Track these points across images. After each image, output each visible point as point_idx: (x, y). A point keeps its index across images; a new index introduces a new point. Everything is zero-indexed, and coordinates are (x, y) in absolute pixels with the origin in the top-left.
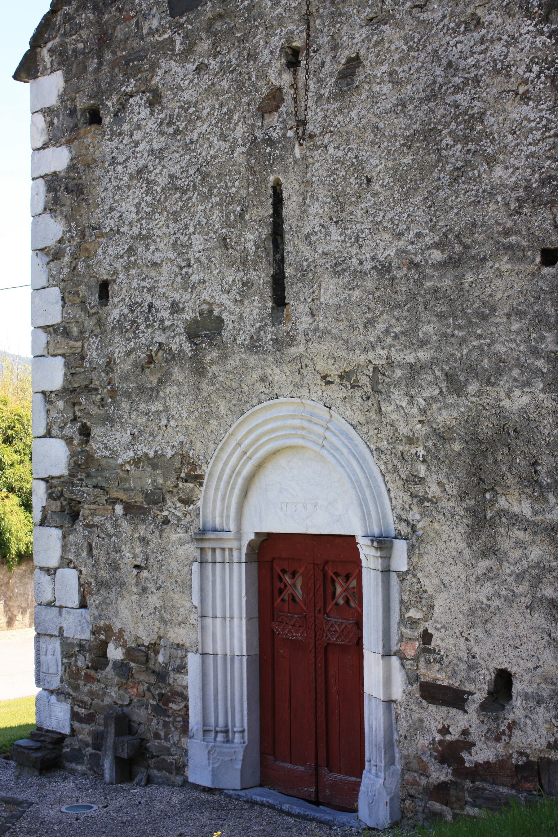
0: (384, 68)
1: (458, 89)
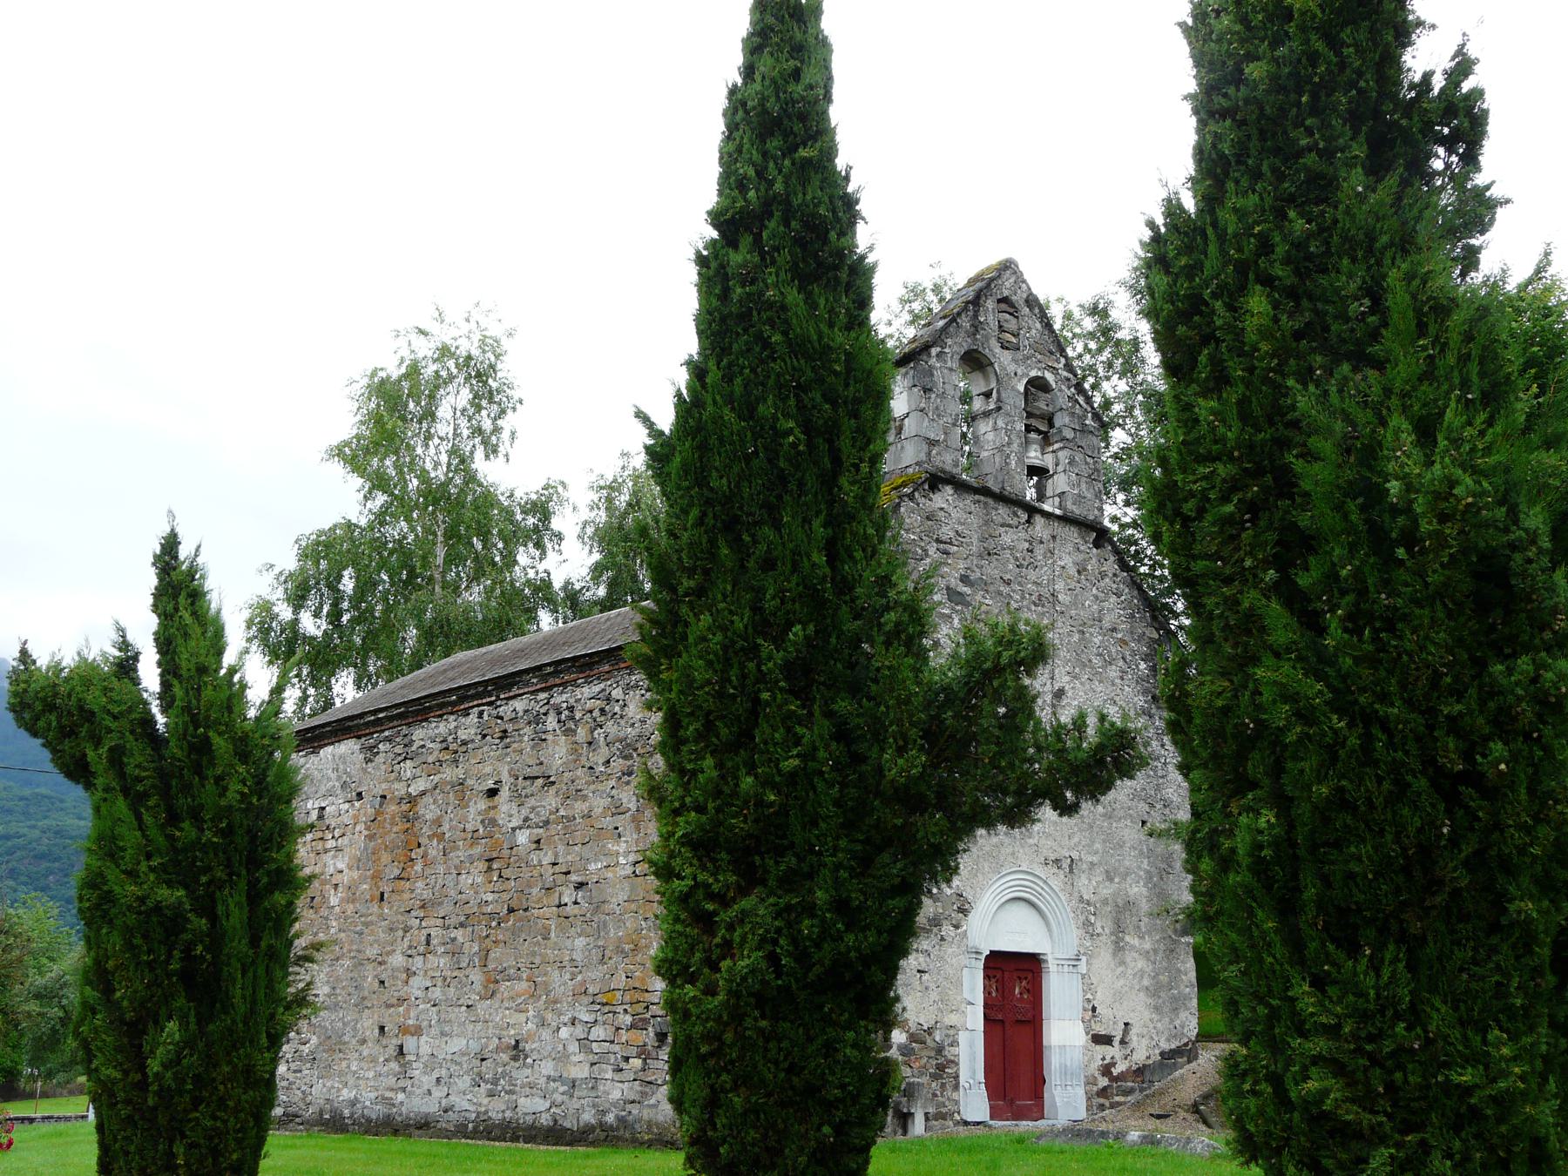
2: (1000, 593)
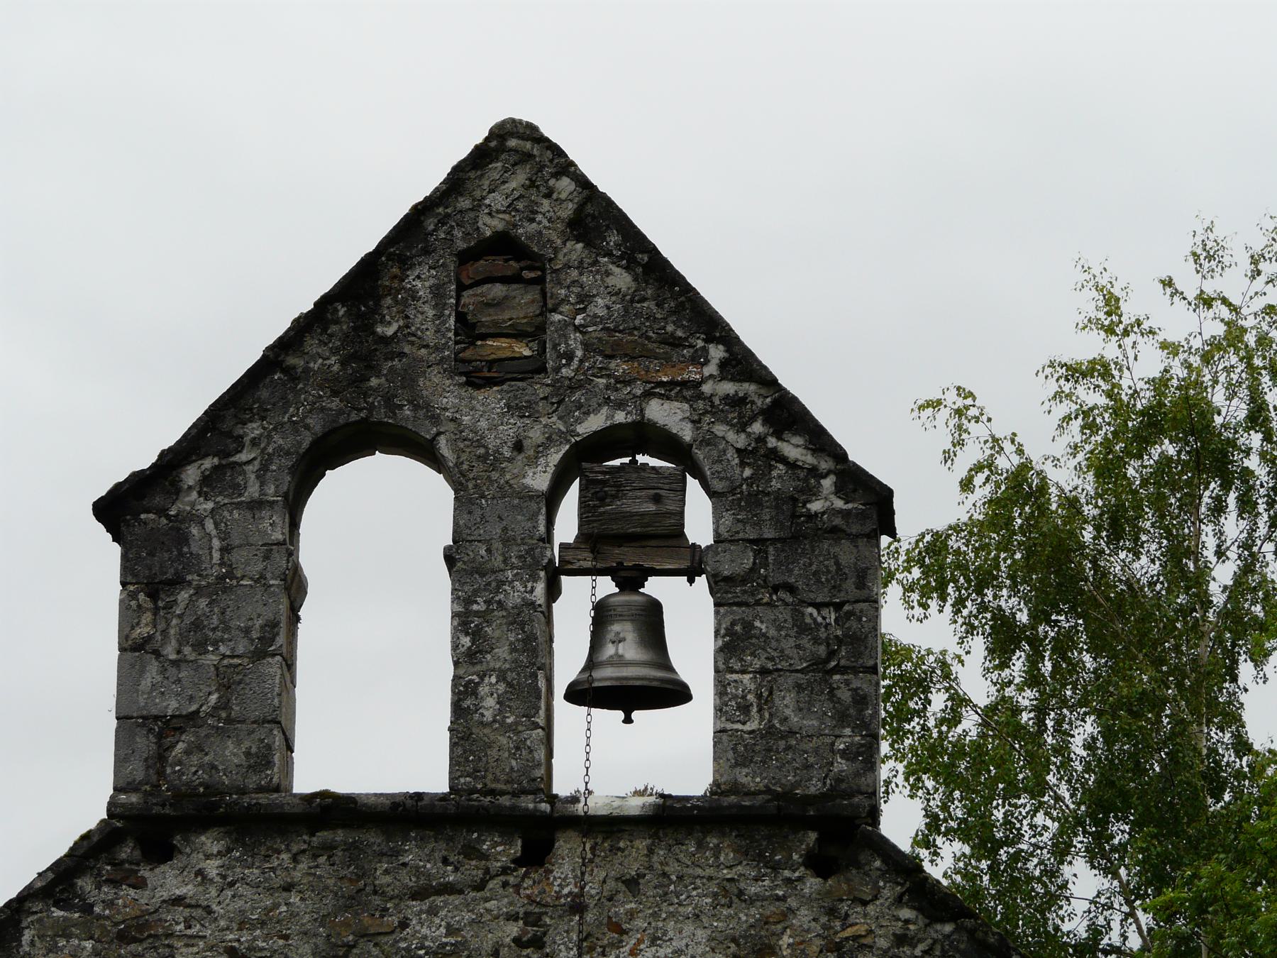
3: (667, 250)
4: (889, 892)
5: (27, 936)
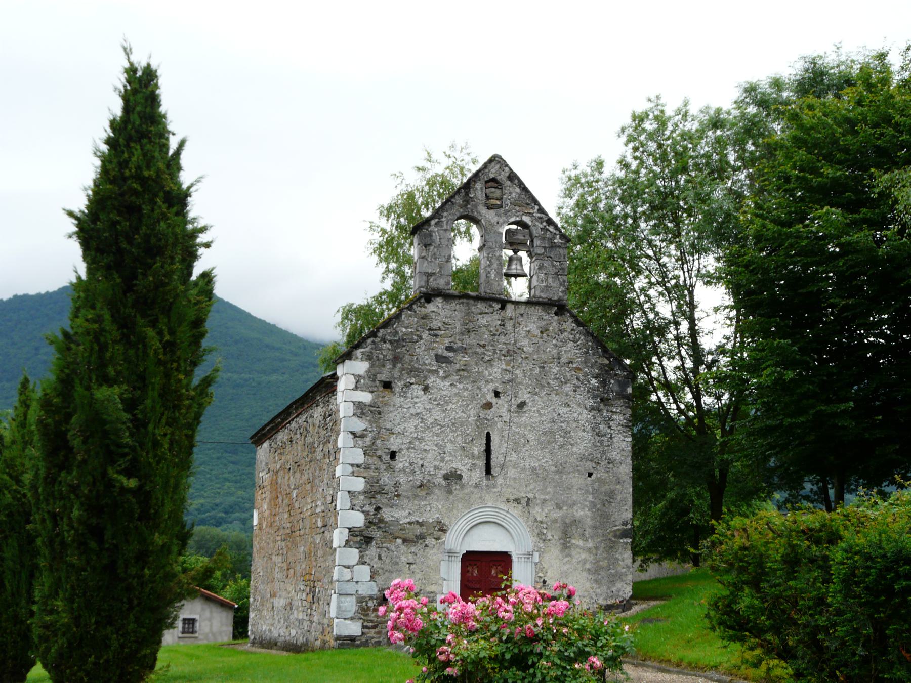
0: (535, 409)
1: (562, 422)
2: (476, 353)
3: (527, 185)
4: (570, 320)
5: (403, 316)
